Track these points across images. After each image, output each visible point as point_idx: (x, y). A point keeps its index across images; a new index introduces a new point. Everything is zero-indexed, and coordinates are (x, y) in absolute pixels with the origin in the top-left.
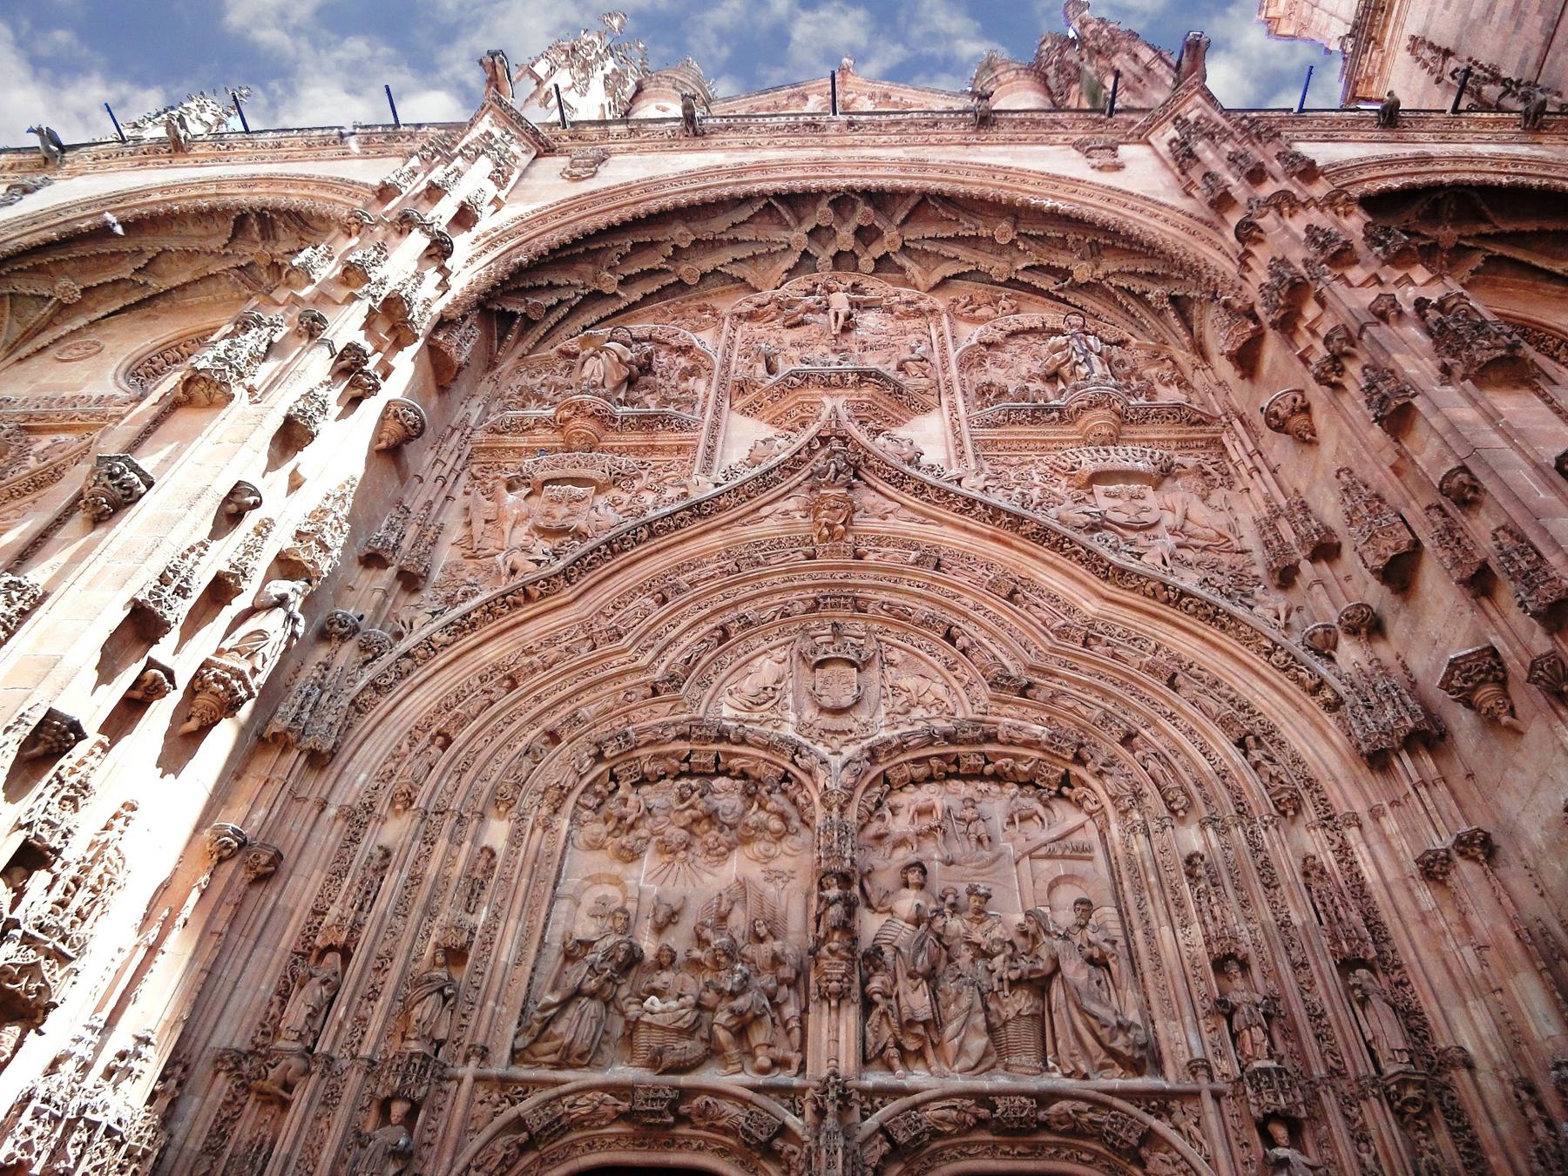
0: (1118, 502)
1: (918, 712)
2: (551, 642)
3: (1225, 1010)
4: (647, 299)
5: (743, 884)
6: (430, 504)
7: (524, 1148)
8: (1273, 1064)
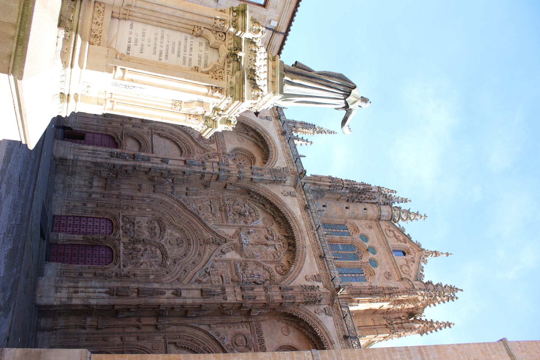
0: (217, 280)
1: (170, 251)
2: (179, 211)
3: (129, 273)
4: (270, 213)
5: (144, 234)
6: (201, 193)
7: (114, 217)
8: (122, 274)
